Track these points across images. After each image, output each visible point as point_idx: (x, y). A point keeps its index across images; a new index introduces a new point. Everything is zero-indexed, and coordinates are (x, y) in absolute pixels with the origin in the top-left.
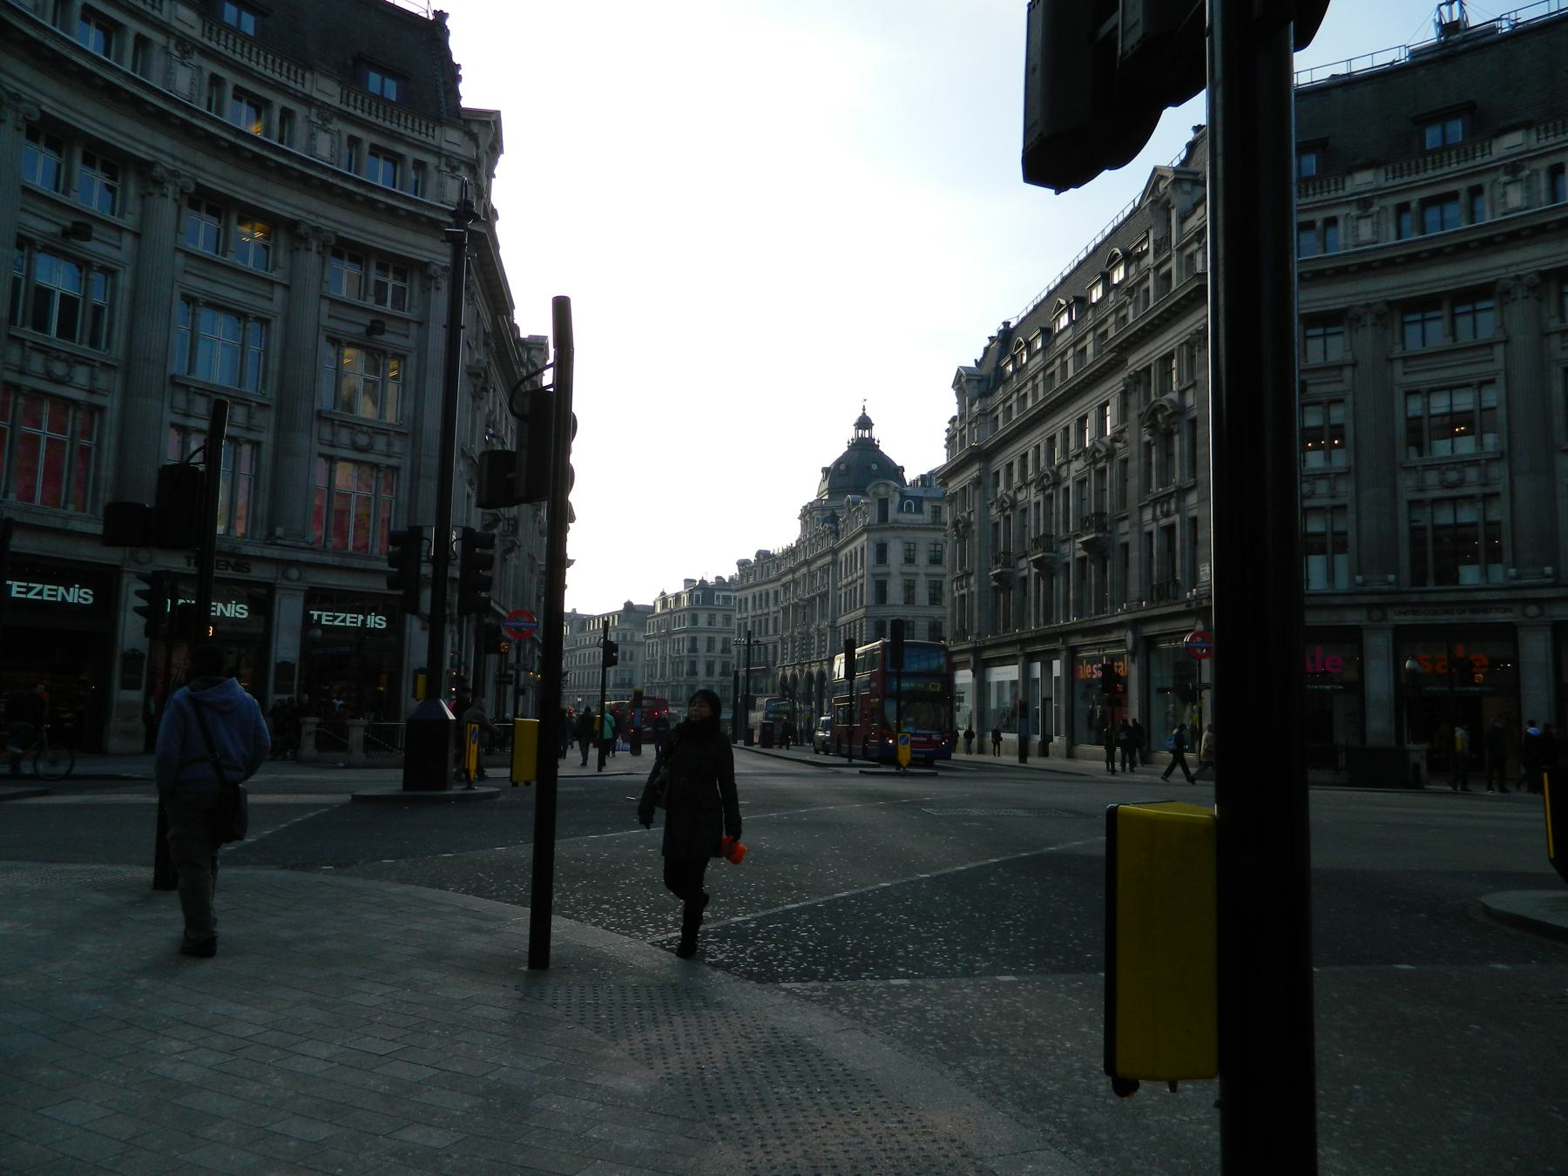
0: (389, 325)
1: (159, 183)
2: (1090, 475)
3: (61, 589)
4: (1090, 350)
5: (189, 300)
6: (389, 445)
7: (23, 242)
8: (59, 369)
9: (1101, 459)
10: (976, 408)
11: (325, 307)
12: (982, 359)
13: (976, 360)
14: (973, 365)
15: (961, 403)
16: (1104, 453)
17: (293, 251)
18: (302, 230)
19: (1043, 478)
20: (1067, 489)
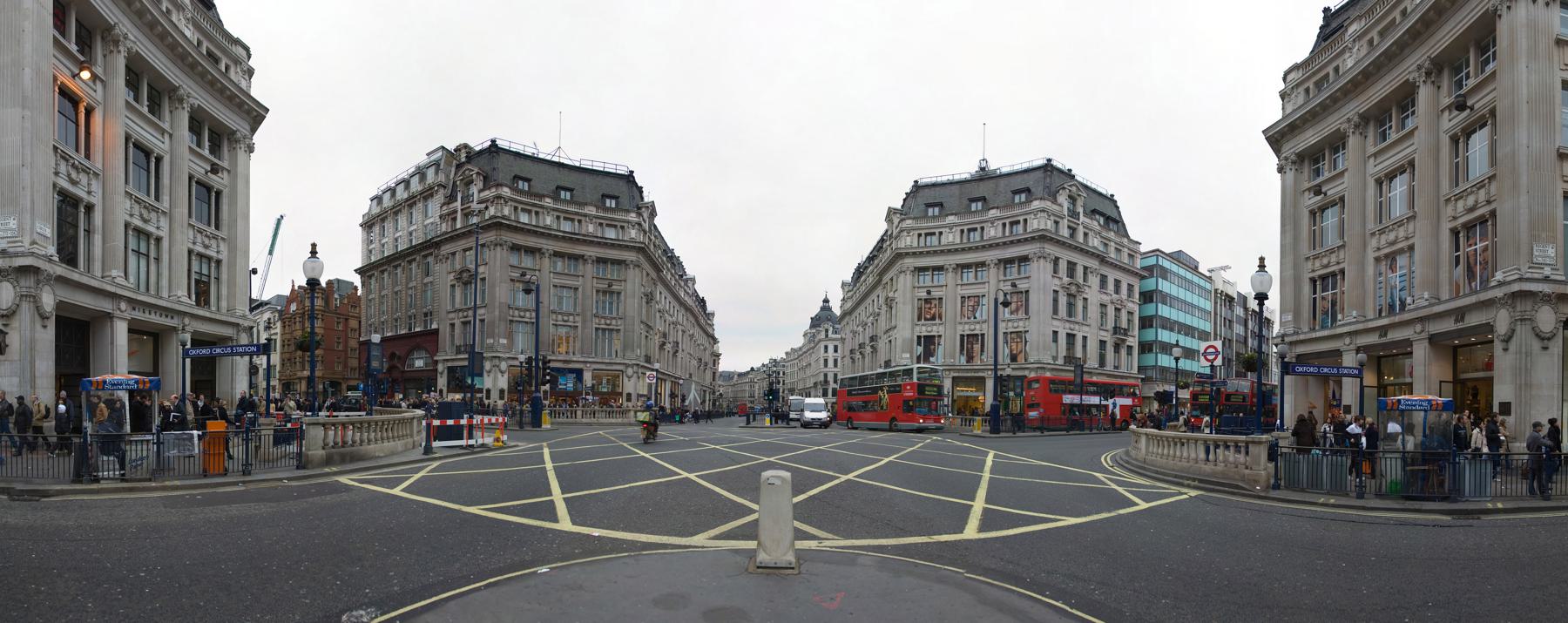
0: (614, 283)
1: (543, 254)
5: (555, 286)
6: (617, 322)
7: (512, 280)
8: (522, 314)
11: (595, 280)
17: (584, 264)
18: (585, 257)
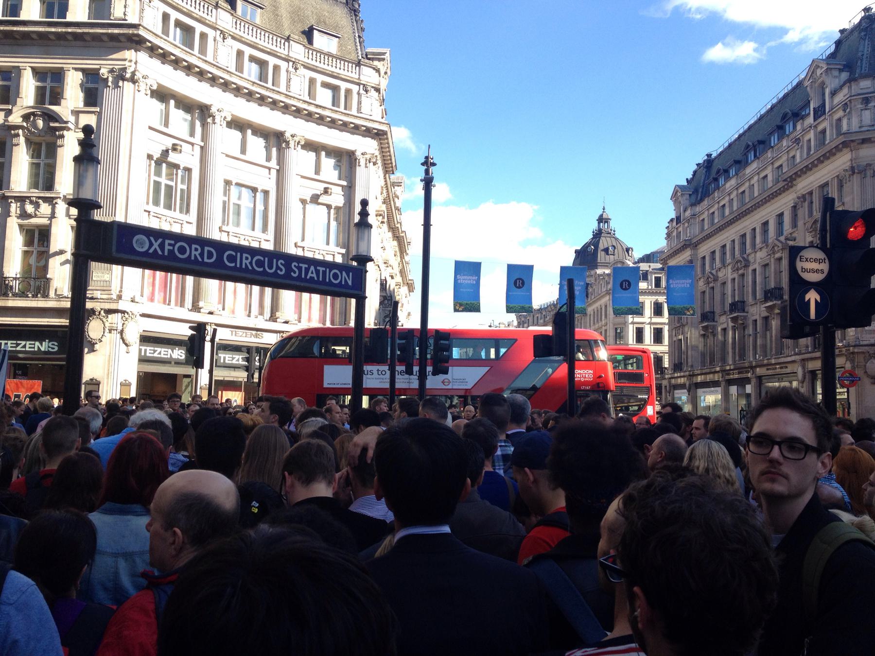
2: (770, 261)
3: (37, 344)
4: (770, 178)
9: (778, 251)
10: (688, 213)
12: (692, 179)
13: (687, 179)
14: (685, 183)
15: (677, 209)
16: (781, 248)
19: (737, 262)
20: (755, 270)
